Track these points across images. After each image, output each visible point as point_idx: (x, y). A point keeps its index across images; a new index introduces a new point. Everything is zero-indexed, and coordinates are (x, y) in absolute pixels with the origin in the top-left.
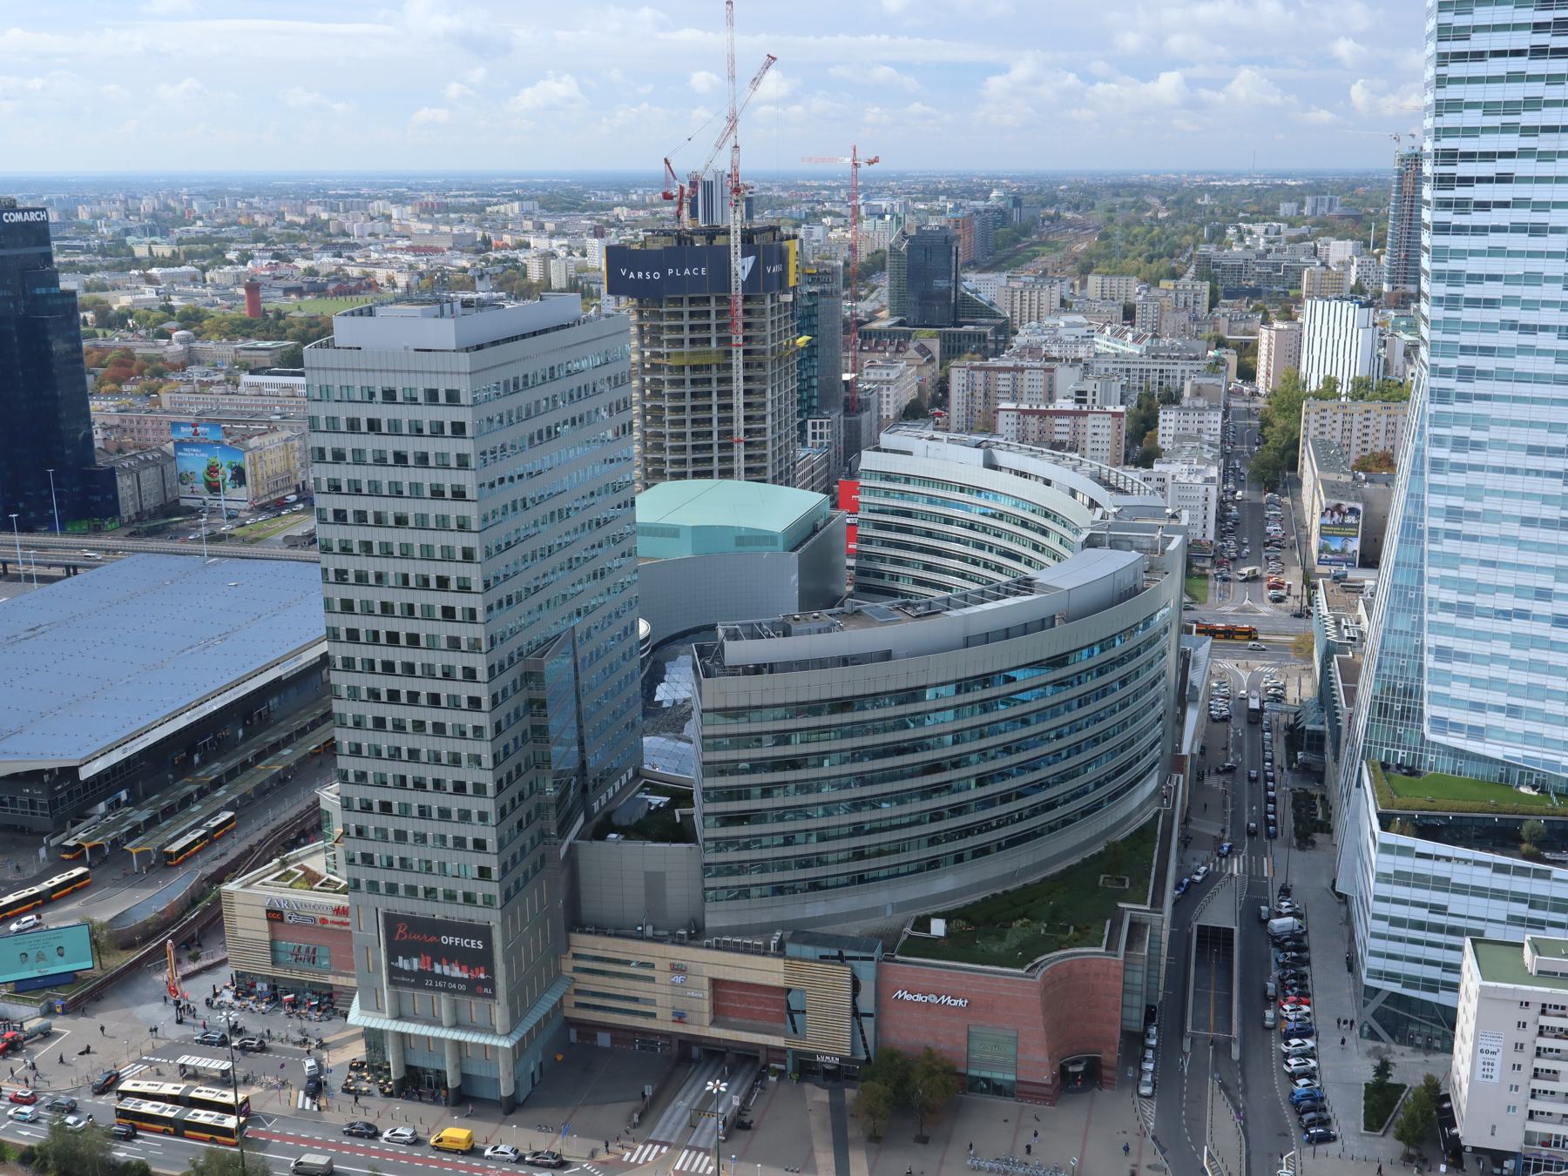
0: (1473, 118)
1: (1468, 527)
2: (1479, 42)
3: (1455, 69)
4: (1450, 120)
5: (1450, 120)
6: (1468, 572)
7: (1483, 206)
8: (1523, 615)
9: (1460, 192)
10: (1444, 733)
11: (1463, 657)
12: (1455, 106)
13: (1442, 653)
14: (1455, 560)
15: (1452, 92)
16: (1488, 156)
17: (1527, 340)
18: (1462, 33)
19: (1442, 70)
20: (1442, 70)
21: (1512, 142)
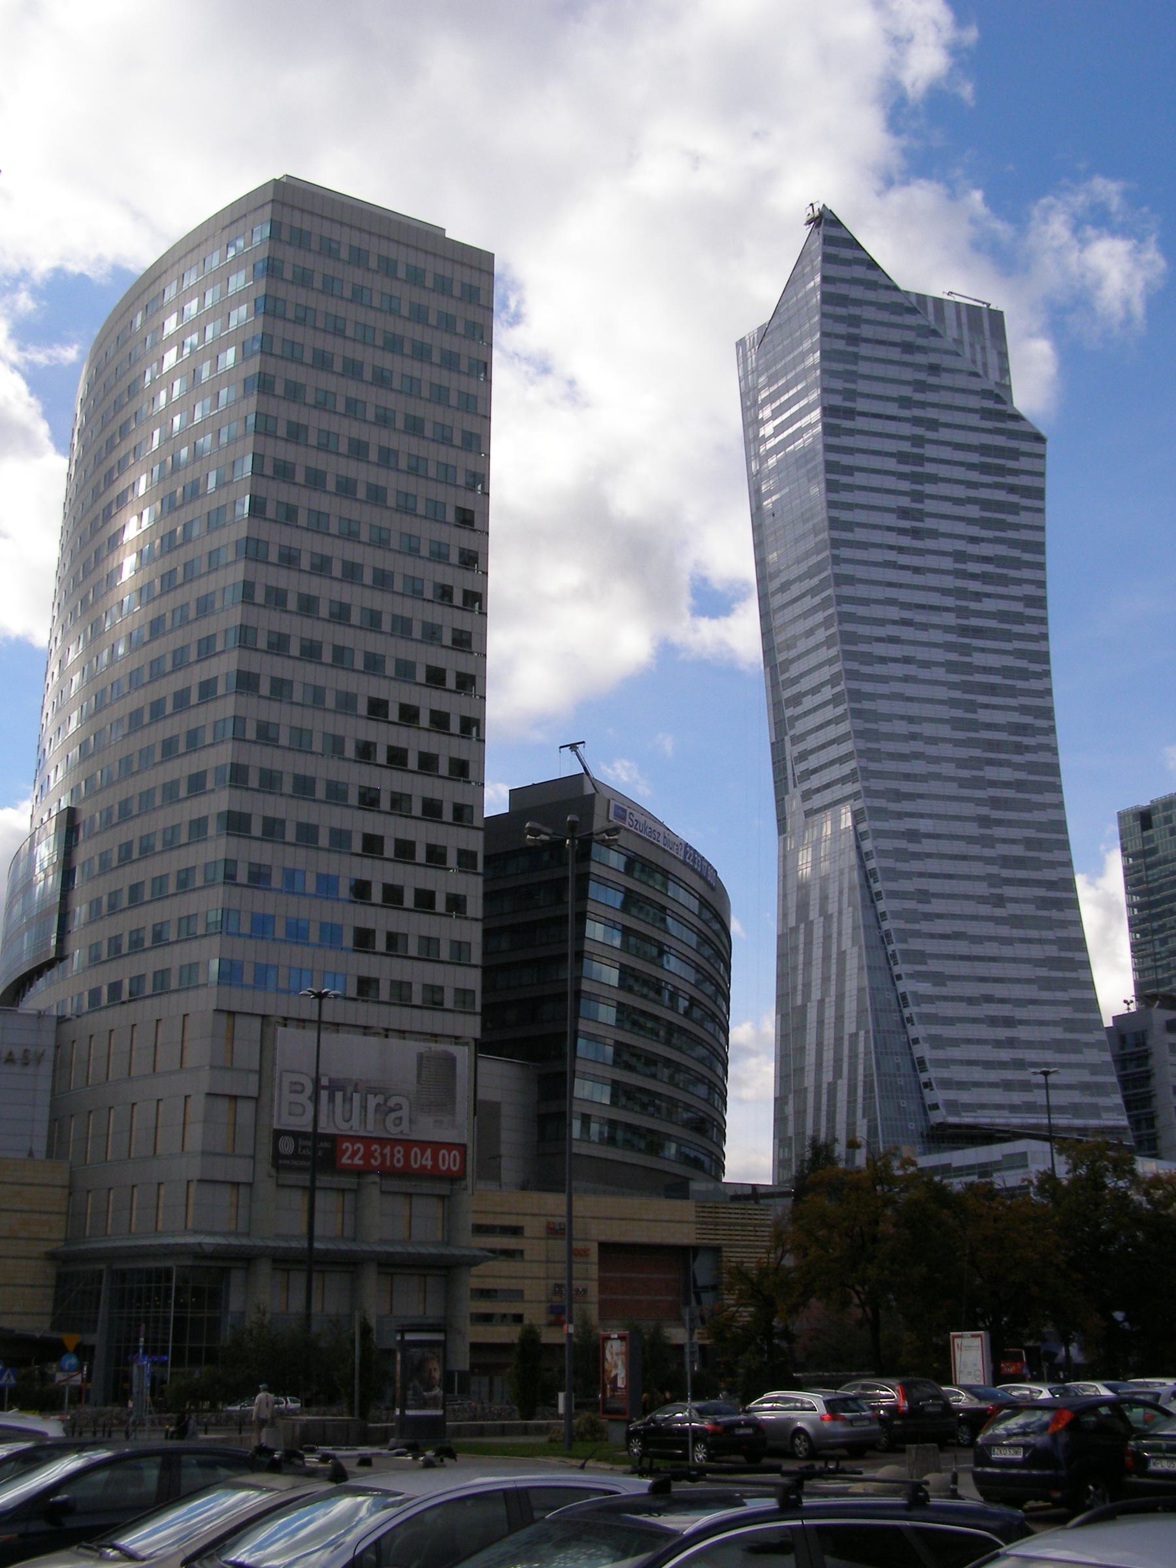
0: (861, 591)
1: (924, 926)
2: (860, 535)
3: (845, 553)
4: (847, 590)
5: (847, 590)
6: (934, 966)
7: (883, 660)
8: (989, 999)
9: (863, 648)
10: (957, 1114)
11: (955, 1042)
12: (850, 580)
13: (937, 1042)
14: (920, 957)
15: (847, 570)
16: (882, 622)
17: (934, 768)
18: (849, 526)
19: (836, 552)
20: (836, 552)
21: (894, 613)
